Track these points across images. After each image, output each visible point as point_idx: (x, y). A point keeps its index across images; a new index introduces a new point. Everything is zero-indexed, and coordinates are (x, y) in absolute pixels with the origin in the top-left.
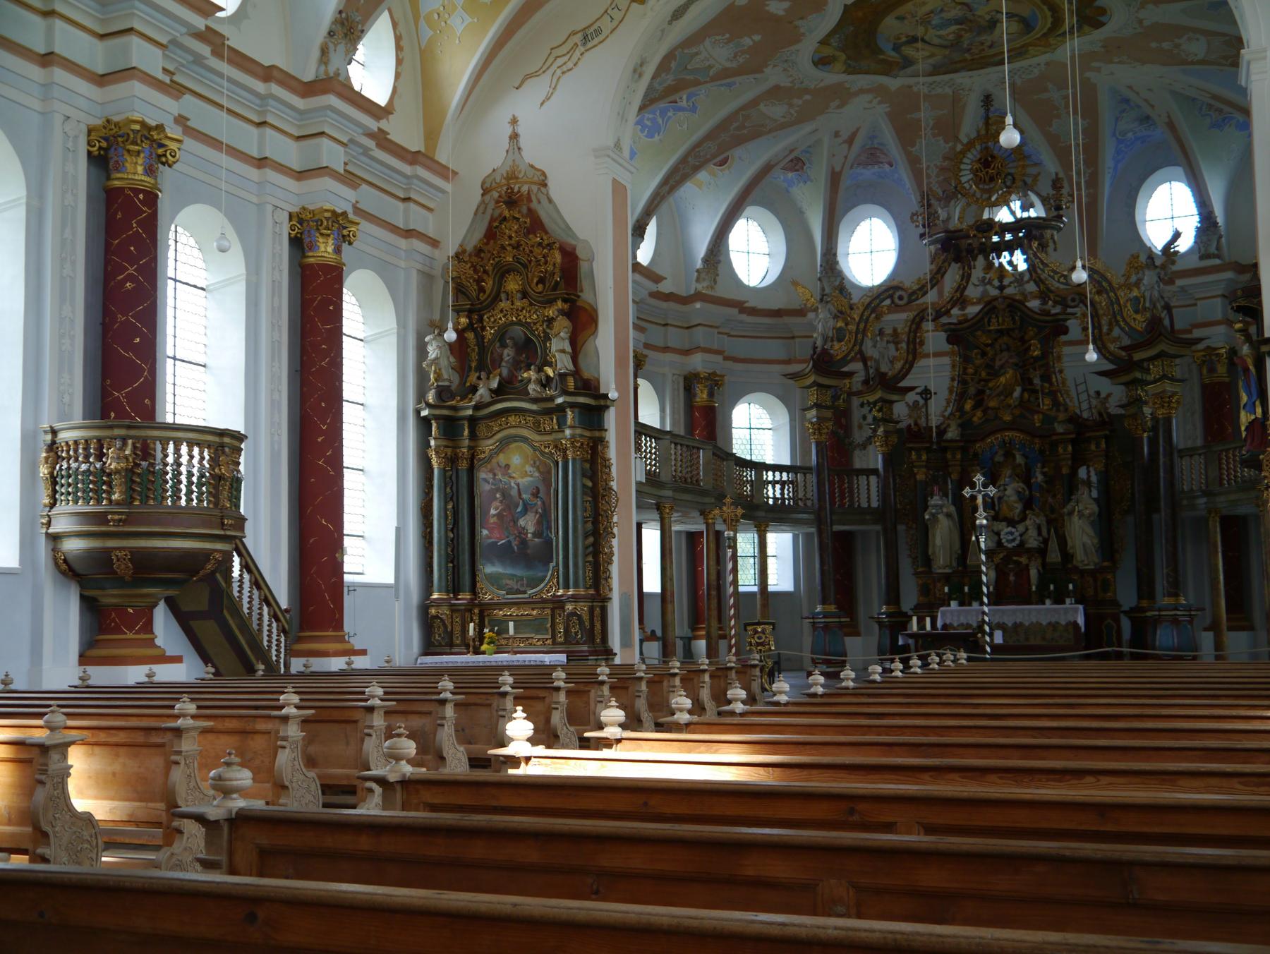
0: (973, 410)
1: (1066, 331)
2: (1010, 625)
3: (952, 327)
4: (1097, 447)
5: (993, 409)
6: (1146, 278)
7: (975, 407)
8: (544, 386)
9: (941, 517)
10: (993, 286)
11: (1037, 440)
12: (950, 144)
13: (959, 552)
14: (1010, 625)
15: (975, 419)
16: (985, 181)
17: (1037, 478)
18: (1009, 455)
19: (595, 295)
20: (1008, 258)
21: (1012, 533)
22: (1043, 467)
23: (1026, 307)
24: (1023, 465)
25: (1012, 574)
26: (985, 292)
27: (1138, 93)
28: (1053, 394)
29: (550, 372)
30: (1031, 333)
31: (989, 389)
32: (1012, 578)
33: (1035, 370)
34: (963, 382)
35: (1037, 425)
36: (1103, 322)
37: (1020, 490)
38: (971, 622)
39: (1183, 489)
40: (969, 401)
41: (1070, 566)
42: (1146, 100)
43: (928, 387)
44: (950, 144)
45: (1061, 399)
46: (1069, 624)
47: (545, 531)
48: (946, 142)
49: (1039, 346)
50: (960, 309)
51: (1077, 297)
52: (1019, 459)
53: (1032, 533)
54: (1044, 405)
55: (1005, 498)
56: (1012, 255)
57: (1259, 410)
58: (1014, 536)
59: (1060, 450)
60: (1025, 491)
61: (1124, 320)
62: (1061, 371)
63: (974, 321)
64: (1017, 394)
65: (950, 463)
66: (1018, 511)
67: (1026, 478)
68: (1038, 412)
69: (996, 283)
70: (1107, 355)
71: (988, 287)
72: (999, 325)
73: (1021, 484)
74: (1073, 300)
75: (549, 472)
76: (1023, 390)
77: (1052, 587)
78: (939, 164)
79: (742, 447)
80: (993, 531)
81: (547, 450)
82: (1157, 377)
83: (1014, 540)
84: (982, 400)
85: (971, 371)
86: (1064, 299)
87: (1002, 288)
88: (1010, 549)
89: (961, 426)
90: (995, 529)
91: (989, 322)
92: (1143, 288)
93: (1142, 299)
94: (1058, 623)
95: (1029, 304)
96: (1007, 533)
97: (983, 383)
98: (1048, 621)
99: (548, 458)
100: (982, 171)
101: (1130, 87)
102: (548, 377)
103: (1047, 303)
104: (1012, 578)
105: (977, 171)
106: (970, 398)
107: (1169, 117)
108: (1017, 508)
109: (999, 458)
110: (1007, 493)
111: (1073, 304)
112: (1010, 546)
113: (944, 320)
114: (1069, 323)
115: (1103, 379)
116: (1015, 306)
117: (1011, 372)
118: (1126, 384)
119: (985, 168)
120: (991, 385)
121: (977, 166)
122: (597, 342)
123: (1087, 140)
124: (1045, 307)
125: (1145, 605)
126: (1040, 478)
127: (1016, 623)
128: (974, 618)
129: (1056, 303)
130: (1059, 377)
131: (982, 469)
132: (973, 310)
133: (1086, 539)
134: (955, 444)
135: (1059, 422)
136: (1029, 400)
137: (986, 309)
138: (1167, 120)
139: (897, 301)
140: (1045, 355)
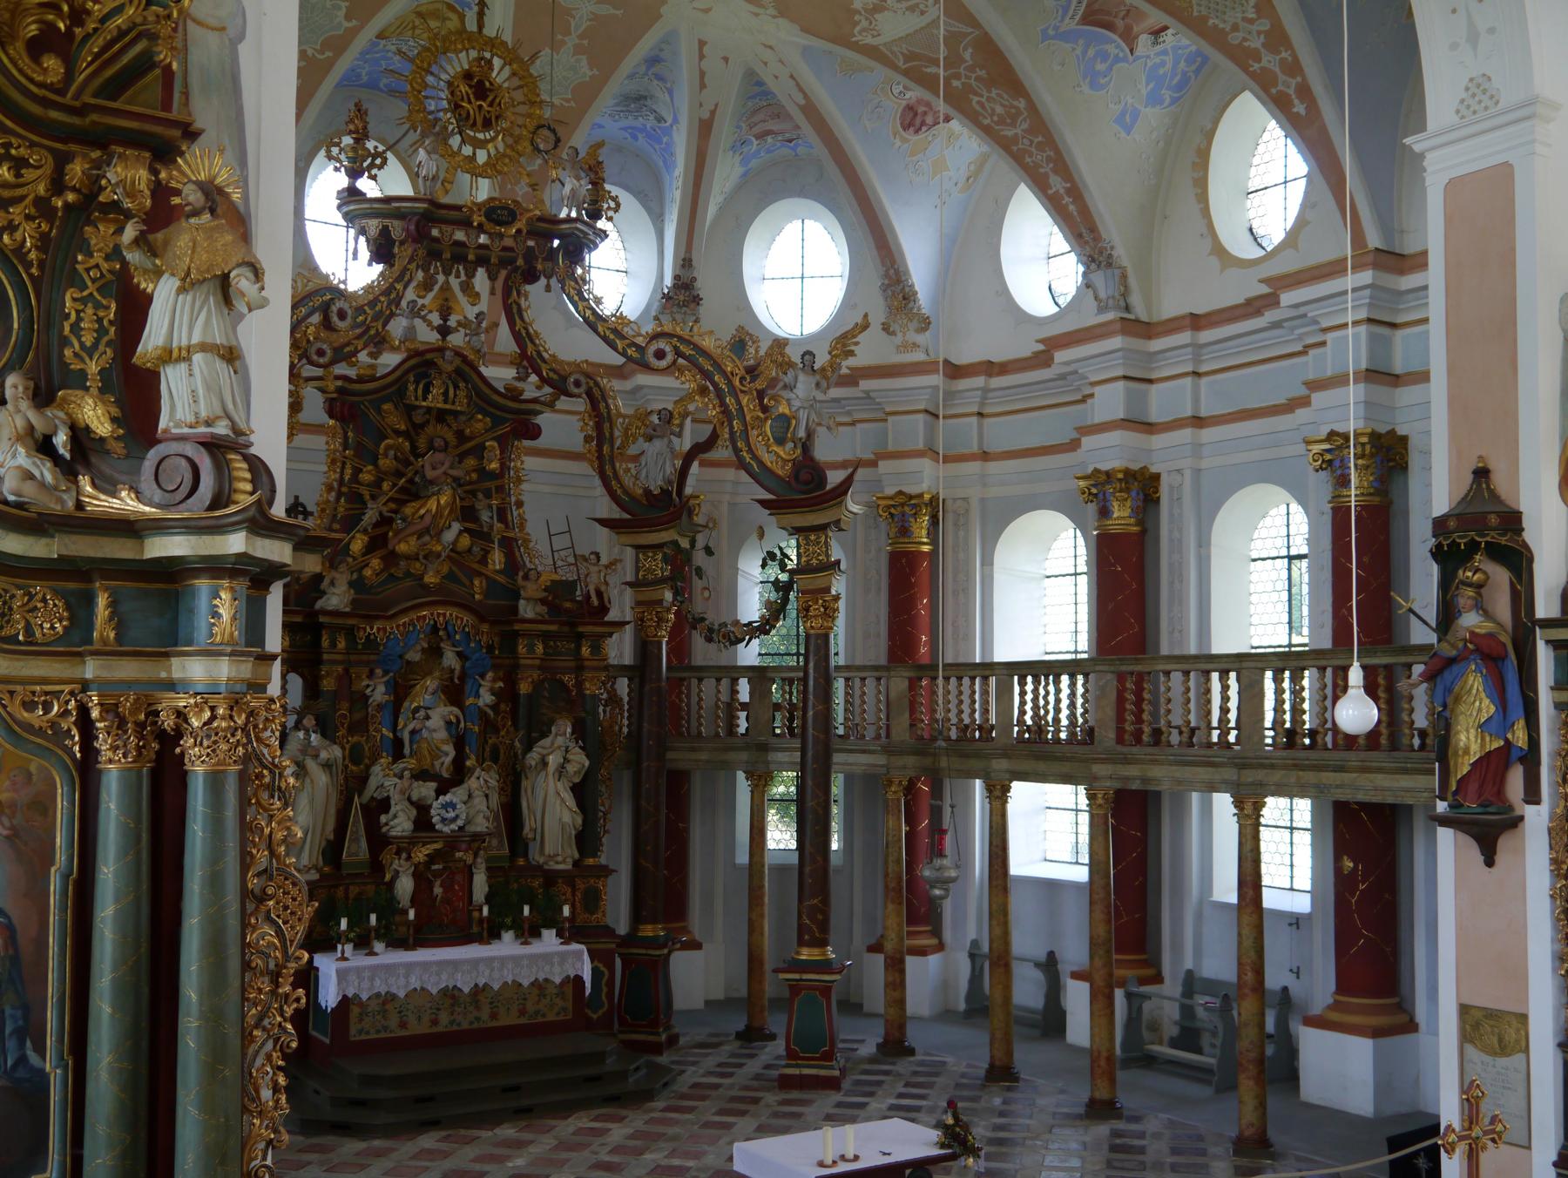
0: (364, 555)
1: (535, 433)
2: (466, 990)
3: (347, 385)
4: (592, 653)
5: (408, 557)
6: (799, 385)
7: (370, 549)
8: (69, 470)
9: (311, 764)
10: (429, 324)
11: (485, 628)
12: (354, 23)
13: (331, 837)
14: (466, 990)
15: (368, 572)
16: (474, 124)
17: (477, 696)
18: (435, 652)
19: (243, 162)
20: (463, 277)
21: (453, 806)
22: (494, 680)
23: (480, 375)
24: (457, 673)
25: (438, 883)
26: (410, 332)
27: (702, 56)
28: (508, 545)
29: (96, 416)
30: (479, 426)
31: (404, 520)
32: (438, 890)
33: (488, 495)
34: (356, 499)
35: (477, 597)
36: (617, 433)
37: (453, 719)
38: (394, 990)
39: (700, 733)
40: (358, 535)
41: (521, 862)
42: (702, 74)
43: (301, 500)
44: (354, 23)
45: (517, 554)
46: (567, 980)
47: (11, 1044)
48: (348, 17)
49: (498, 452)
50: (371, 355)
51: (583, 379)
52: (450, 659)
53: (479, 803)
54: (497, 559)
55: (425, 733)
56: (471, 275)
57: (1520, 737)
58: (457, 812)
59: (521, 649)
60: (458, 721)
61: (750, 451)
62: (520, 504)
63: (381, 382)
64: (449, 536)
65: (325, 657)
66: (448, 760)
67: (454, 693)
68: (480, 574)
69: (436, 319)
70: (619, 492)
71: (418, 322)
72: (446, 402)
73: (456, 710)
74: (577, 384)
75: (43, 806)
76: (461, 532)
77: (526, 910)
78: (310, 52)
79: (1278, 859)
80: (409, 799)
81: (37, 717)
82: (814, 562)
83: (457, 817)
84: (384, 537)
85: (366, 477)
86: (564, 379)
87: (444, 331)
88: (448, 836)
89: (351, 584)
90: (414, 798)
91: (427, 391)
92: (796, 403)
93: (794, 422)
94: (546, 980)
95: (489, 372)
96: (445, 806)
97: (392, 506)
98: (533, 979)
99: (42, 751)
100: (470, 102)
101: (702, 44)
102: (80, 436)
103: (528, 376)
104: (438, 890)
105: (462, 99)
106: (365, 531)
107: (713, 113)
108: (447, 754)
109: (414, 656)
110: (428, 723)
111: (576, 391)
112: (446, 829)
113: (341, 369)
114: (539, 420)
115: (606, 530)
116: (466, 371)
117: (449, 492)
118: (638, 548)
119: (477, 99)
120: (408, 510)
121: (464, 88)
122: (240, 328)
123: (573, 104)
124: (519, 385)
125: (651, 934)
126: (486, 698)
127: (476, 985)
128: (402, 981)
129: (544, 381)
130: (515, 514)
131: (386, 673)
132: (390, 360)
133: (567, 818)
134: (340, 621)
135: (528, 599)
136: (469, 550)
137: (407, 365)
138: (706, 115)
139: (335, 319)
140: (504, 467)
